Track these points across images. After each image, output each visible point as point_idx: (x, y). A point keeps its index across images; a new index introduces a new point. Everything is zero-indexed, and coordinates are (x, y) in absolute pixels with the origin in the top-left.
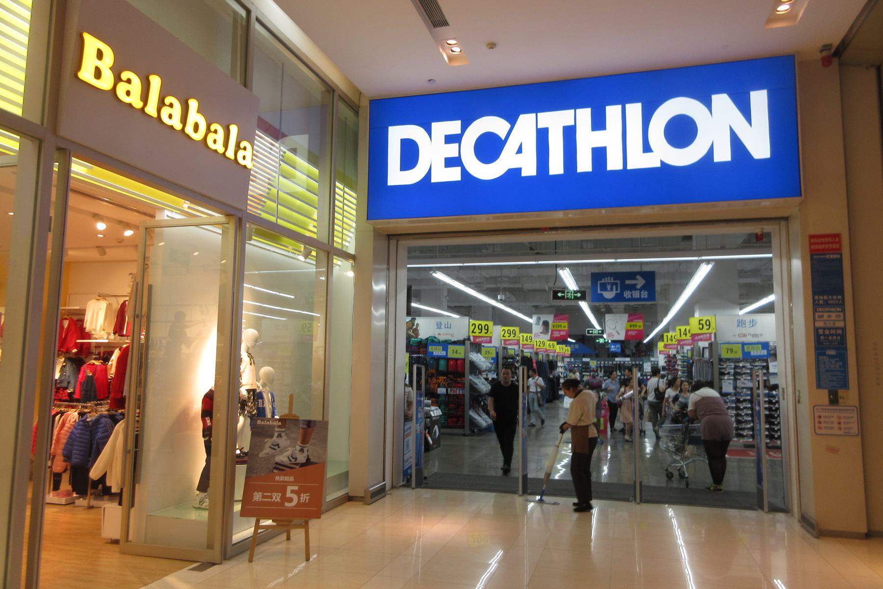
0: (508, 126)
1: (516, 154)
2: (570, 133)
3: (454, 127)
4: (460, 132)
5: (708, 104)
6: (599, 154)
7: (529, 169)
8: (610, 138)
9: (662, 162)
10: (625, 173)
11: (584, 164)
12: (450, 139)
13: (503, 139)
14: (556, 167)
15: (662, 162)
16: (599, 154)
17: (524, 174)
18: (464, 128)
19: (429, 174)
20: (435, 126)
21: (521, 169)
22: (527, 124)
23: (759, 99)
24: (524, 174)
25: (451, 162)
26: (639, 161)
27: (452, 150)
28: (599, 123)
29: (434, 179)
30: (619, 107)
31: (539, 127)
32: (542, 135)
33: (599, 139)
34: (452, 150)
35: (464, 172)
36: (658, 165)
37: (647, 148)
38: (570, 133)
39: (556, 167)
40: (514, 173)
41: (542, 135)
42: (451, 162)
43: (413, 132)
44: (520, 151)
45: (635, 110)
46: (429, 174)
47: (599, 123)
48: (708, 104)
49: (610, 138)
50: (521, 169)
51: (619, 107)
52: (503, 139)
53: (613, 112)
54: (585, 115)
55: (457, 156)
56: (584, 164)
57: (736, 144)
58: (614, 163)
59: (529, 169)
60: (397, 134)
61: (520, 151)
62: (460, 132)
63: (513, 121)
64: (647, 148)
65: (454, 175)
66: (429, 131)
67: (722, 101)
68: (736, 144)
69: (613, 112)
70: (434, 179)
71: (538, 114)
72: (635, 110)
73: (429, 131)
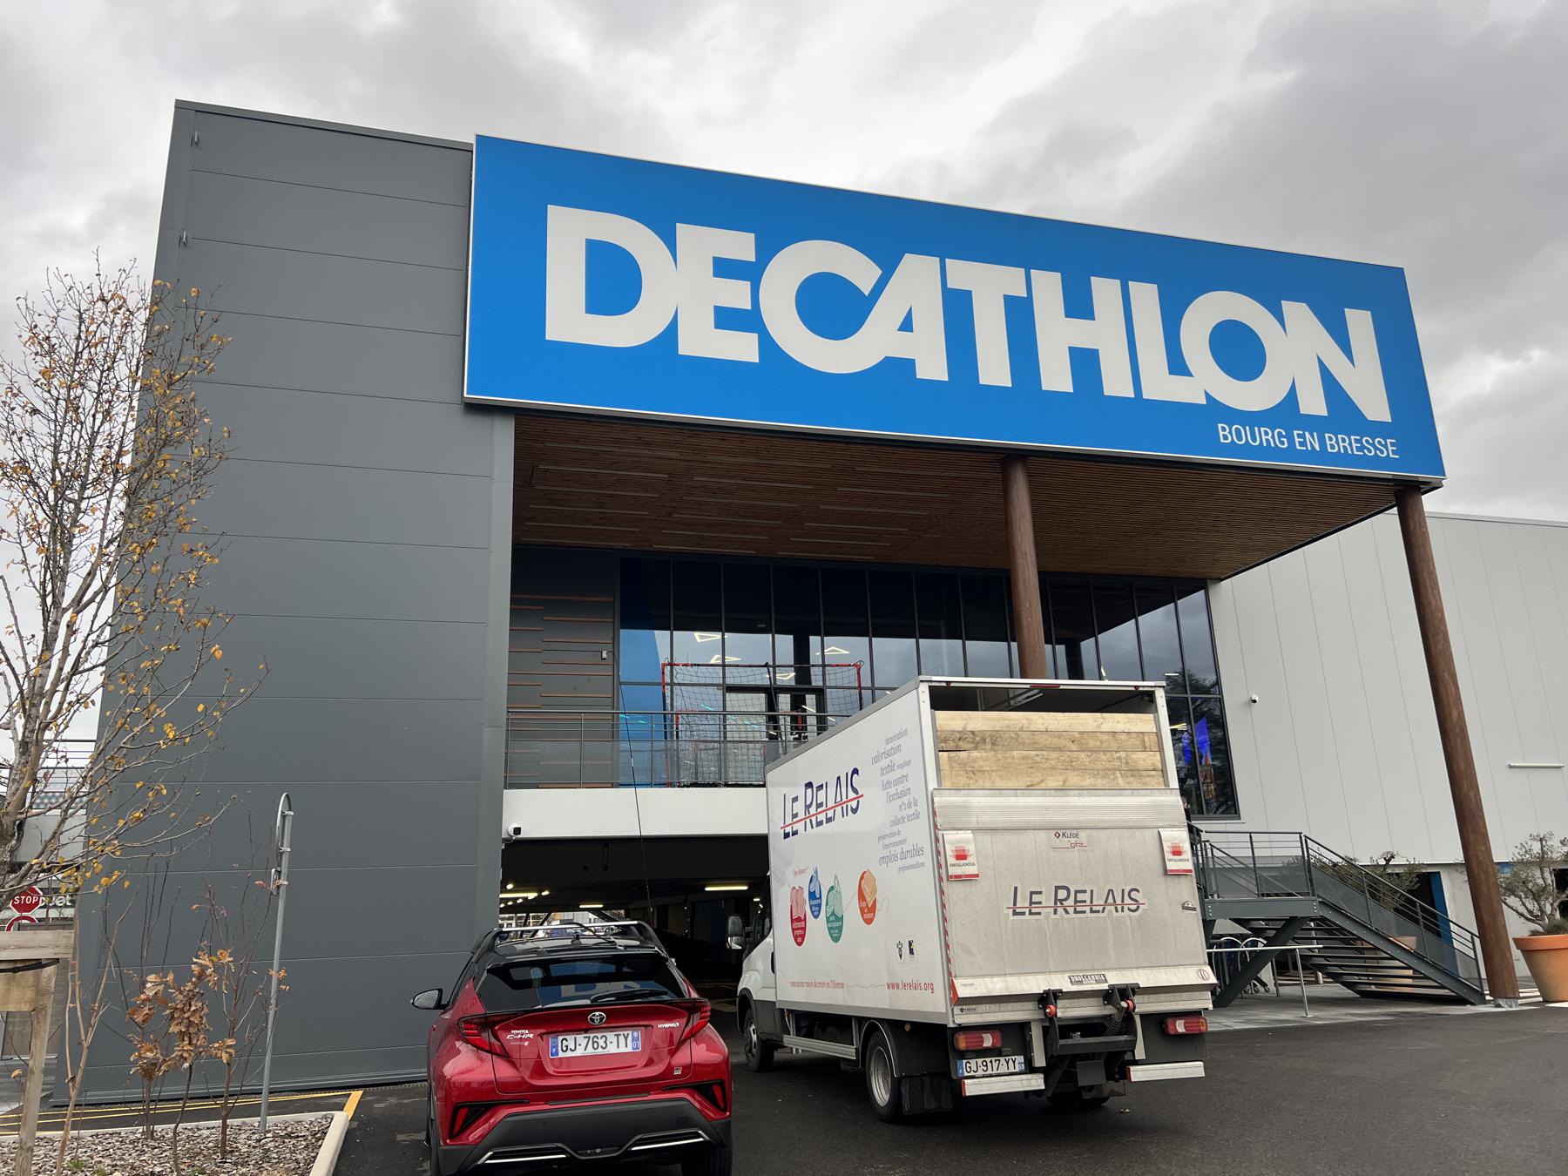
0: (877, 272)
1: (899, 330)
2: (1019, 314)
3: (741, 246)
6: (1085, 362)
7: (933, 366)
10: (1139, 408)
11: (1056, 376)
12: (725, 268)
14: (994, 368)
15: (1208, 396)
16: (1085, 362)
18: (766, 251)
19: (672, 329)
20: (682, 230)
21: (909, 364)
24: (922, 373)
25: (726, 319)
26: (1161, 386)
27: (736, 294)
29: (688, 346)
32: (958, 307)
33: (1081, 333)
34: (736, 294)
35: (767, 344)
37: (1178, 365)
38: (1019, 314)
39: (994, 368)
40: (897, 370)
41: (958, 307)
42: (726, 319)
44: (907, 325)
46: (672, 329)
47: (1079, 305)
50: (909, 364)
51: (1115, 284)
53: (1105, 290)
54: (1048, 288)
56: (1056, 376)
58: (1116, 383)
59: (933, 366)
61: (907, 325)
63: (888, 267)
64: (1178, 365)
65: (742, 348)
66: (671, 244)
69: (1105, 290)
70: (688, 346)
72: (1146, 296)
73: (671, 243)
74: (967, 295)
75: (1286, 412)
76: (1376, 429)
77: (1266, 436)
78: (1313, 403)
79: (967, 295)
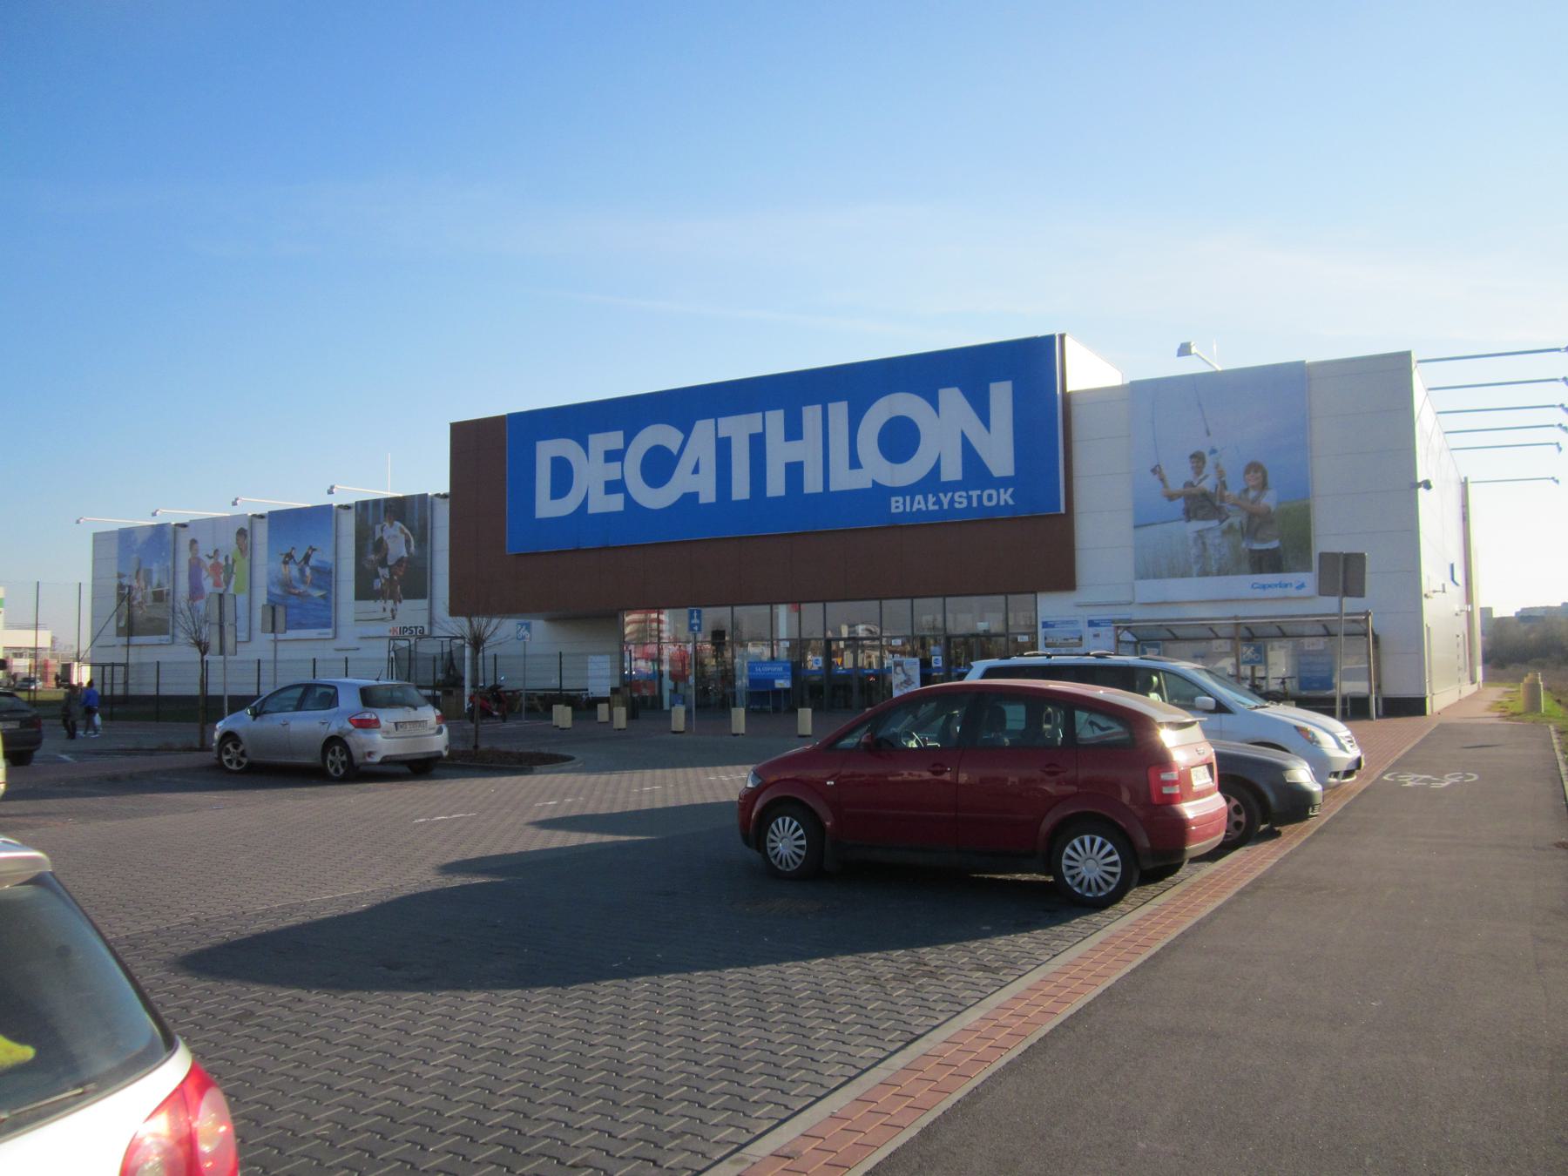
0: (680, 436)
2: (758, 443)
3: (615, 440)
4: (620, 446)
5: (934, 403)
6: (794, 471)
7: (708, 495)
8: (807, 451)
9: (873, 481)
11: (776, 486)
13: (675, 451)
14: (741, 489)
15: (873, 481)
16: (794, 471)
17: (702, 500)
18: (628, 441)
21: (695, 495)
22: (704, 431)
23: (1001, 395)
24: (702, 500)
25: (614, 487)
26: (844, 480)
27: (613, 472)
28: (794, 431)
29: (591, 511)
30: (818, 408)
31: (720, 435)
32: (724, 447)
35: (629, 500)
36: (870, 485)
37: (855, 463)
38: (758, 443)
39: (741, 489)
40: (690, 498)
43: (565, 447)
44: (696, 470)
45: (839, 412)
47: (794, 431)
48: (934, 403)
49: (807, 451)
50: (695, 495)
51: (818, 408)
52: (675, 451)
55: (620, 477)
56: (776, 486)
57: (970, 454)
59: (708, 495)
60: (546, 451)
61: (696, 470)
62: (620, 446)
63: (687, 431)
64: (855, 463)
65: (616, 503)
66: (585, 445)
67: (952, 398)
68: (970, 454)
69: (811, 414)
70: (592, 510)
71: (720, 420)
72: (839, 412)
73: (585, 445)
74: (728, 439)
75: (932, 482)
76: (1003, 482)
77: (919, 503)
78: (952, 471)
79: (728, 439)
